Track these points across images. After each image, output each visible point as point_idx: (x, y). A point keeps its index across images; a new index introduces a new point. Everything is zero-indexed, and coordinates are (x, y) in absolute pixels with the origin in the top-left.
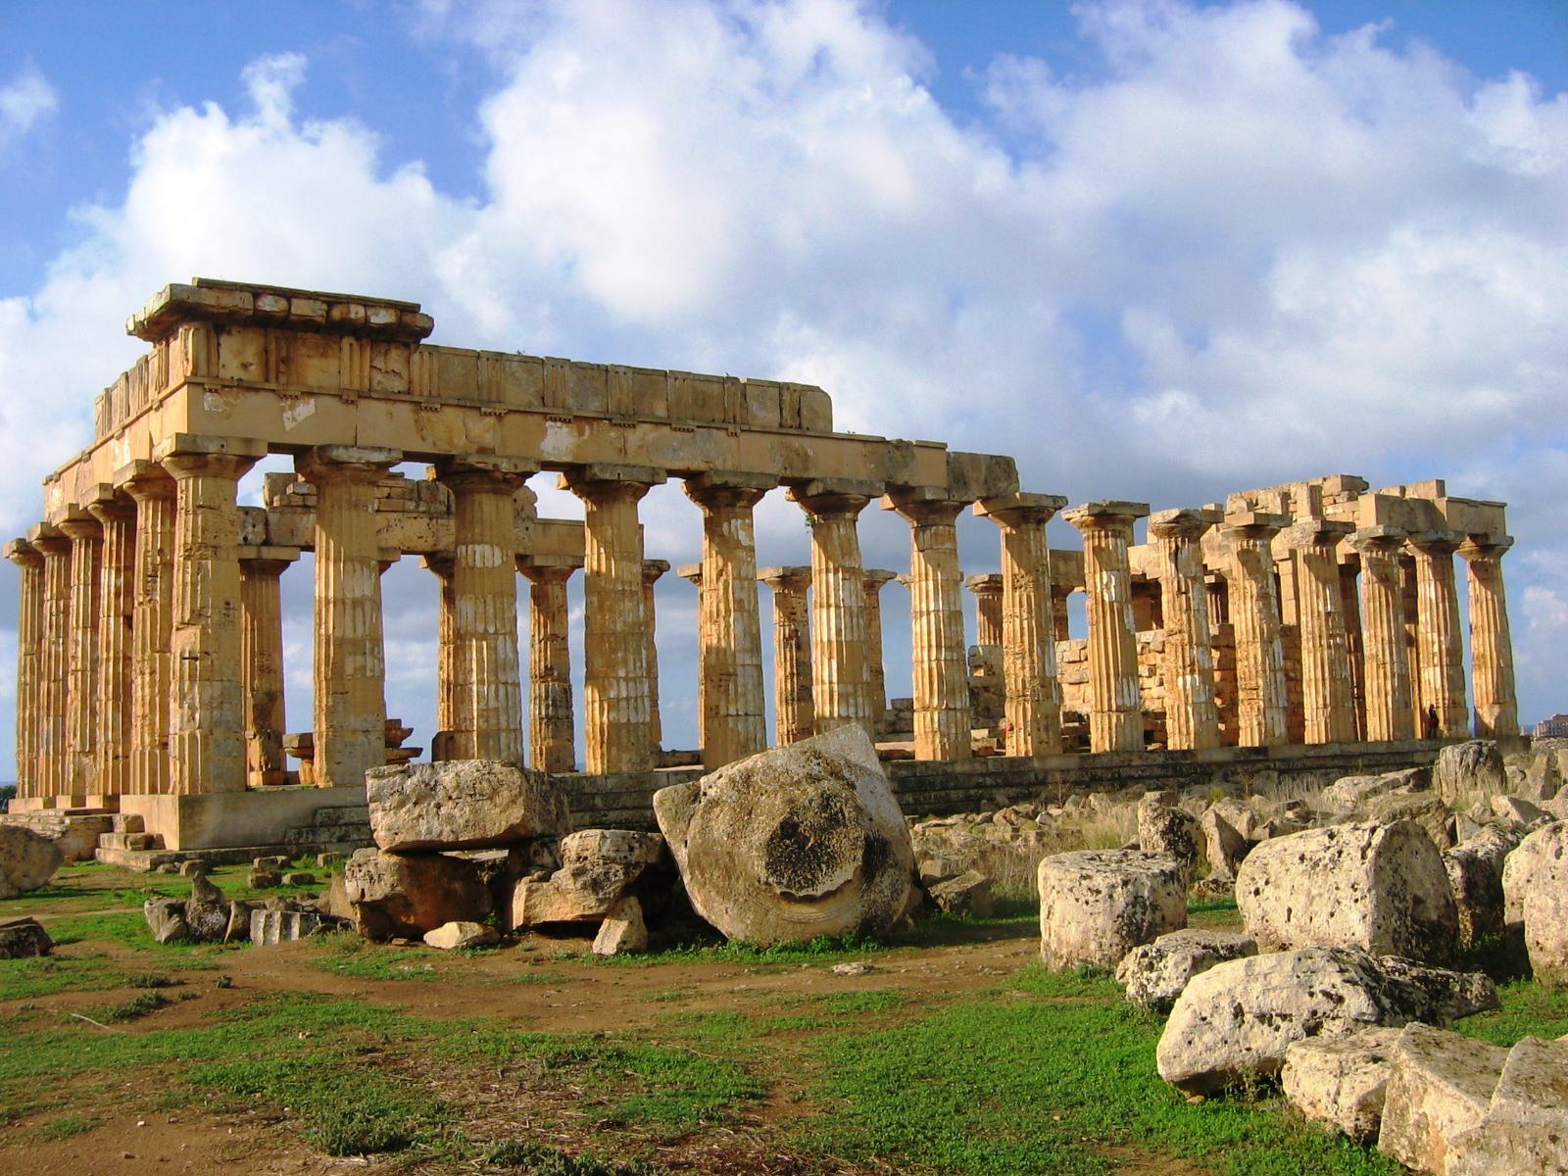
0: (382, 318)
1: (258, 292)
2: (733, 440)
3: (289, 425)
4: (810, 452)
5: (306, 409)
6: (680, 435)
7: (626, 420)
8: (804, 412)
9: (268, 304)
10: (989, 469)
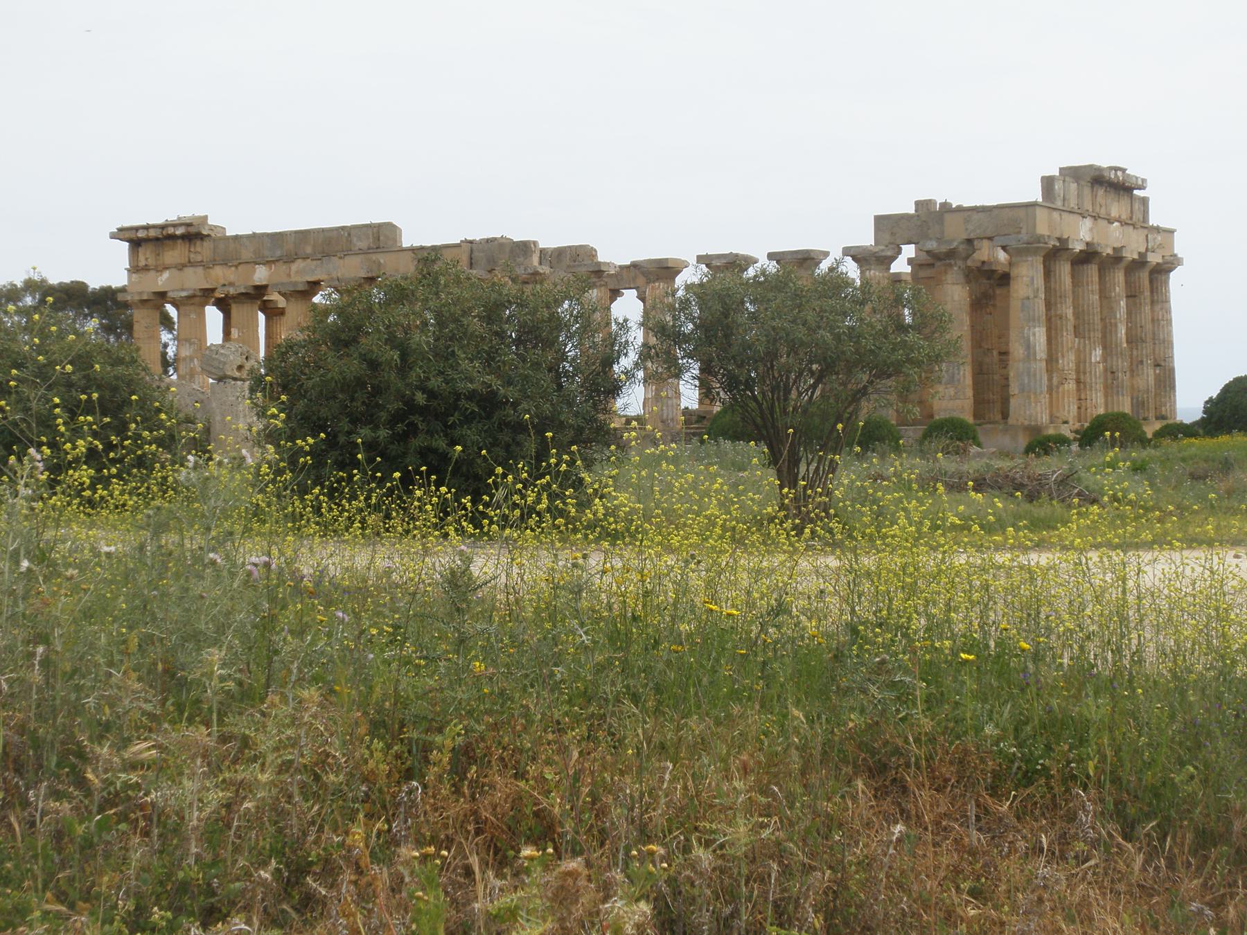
0: (179, 231)
1: (137, 229)
2: (341, 261)
3: (160, 283)
4: (382, 261)
5: (166, 275)
6: (315, 262)
7: (289, 259)
8: (381, 238)
9: (141, 234)
10: (512, 251)
